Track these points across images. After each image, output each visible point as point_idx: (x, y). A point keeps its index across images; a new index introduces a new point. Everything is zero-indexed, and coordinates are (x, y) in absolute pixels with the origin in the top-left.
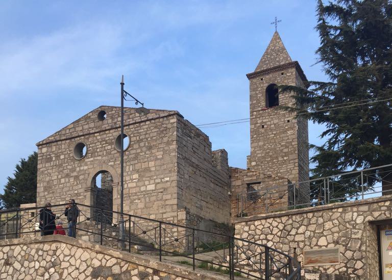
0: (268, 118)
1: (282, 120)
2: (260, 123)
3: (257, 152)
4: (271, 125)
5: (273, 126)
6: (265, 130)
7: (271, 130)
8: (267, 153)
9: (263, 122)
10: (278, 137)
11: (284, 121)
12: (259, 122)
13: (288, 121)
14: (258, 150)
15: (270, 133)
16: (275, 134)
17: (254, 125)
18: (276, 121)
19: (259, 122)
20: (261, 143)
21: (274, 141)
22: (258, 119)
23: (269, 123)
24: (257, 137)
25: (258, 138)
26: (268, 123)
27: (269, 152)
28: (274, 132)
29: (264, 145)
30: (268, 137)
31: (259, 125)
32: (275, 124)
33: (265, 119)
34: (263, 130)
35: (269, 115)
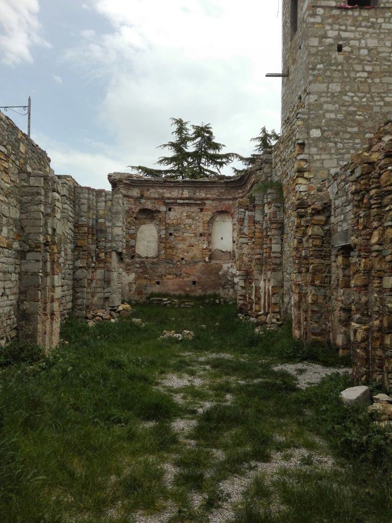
0: (352, 31)
4: (360, 48)
5: (364, 52)
6: (347, 58)
7: (361, 61)
9: (339, 38)
10: (377, 80)
12: (331, 34)
14: (327, 102)
15: (358, 68)
16: (369, 72)
18: (372, 43)
20: (335, 87)
21: (366, 89)
22: (328, 27)
23: (356, 43)
24: (325, 70)
25: (328, 73)
26: (352, 43)
28: (369, 68)
29: (343, 93)
30: (353, 75)
31: (329, 41)
32: (370, 50)
33: (346, 31)
34: (340, 57)
35: (356, 24)
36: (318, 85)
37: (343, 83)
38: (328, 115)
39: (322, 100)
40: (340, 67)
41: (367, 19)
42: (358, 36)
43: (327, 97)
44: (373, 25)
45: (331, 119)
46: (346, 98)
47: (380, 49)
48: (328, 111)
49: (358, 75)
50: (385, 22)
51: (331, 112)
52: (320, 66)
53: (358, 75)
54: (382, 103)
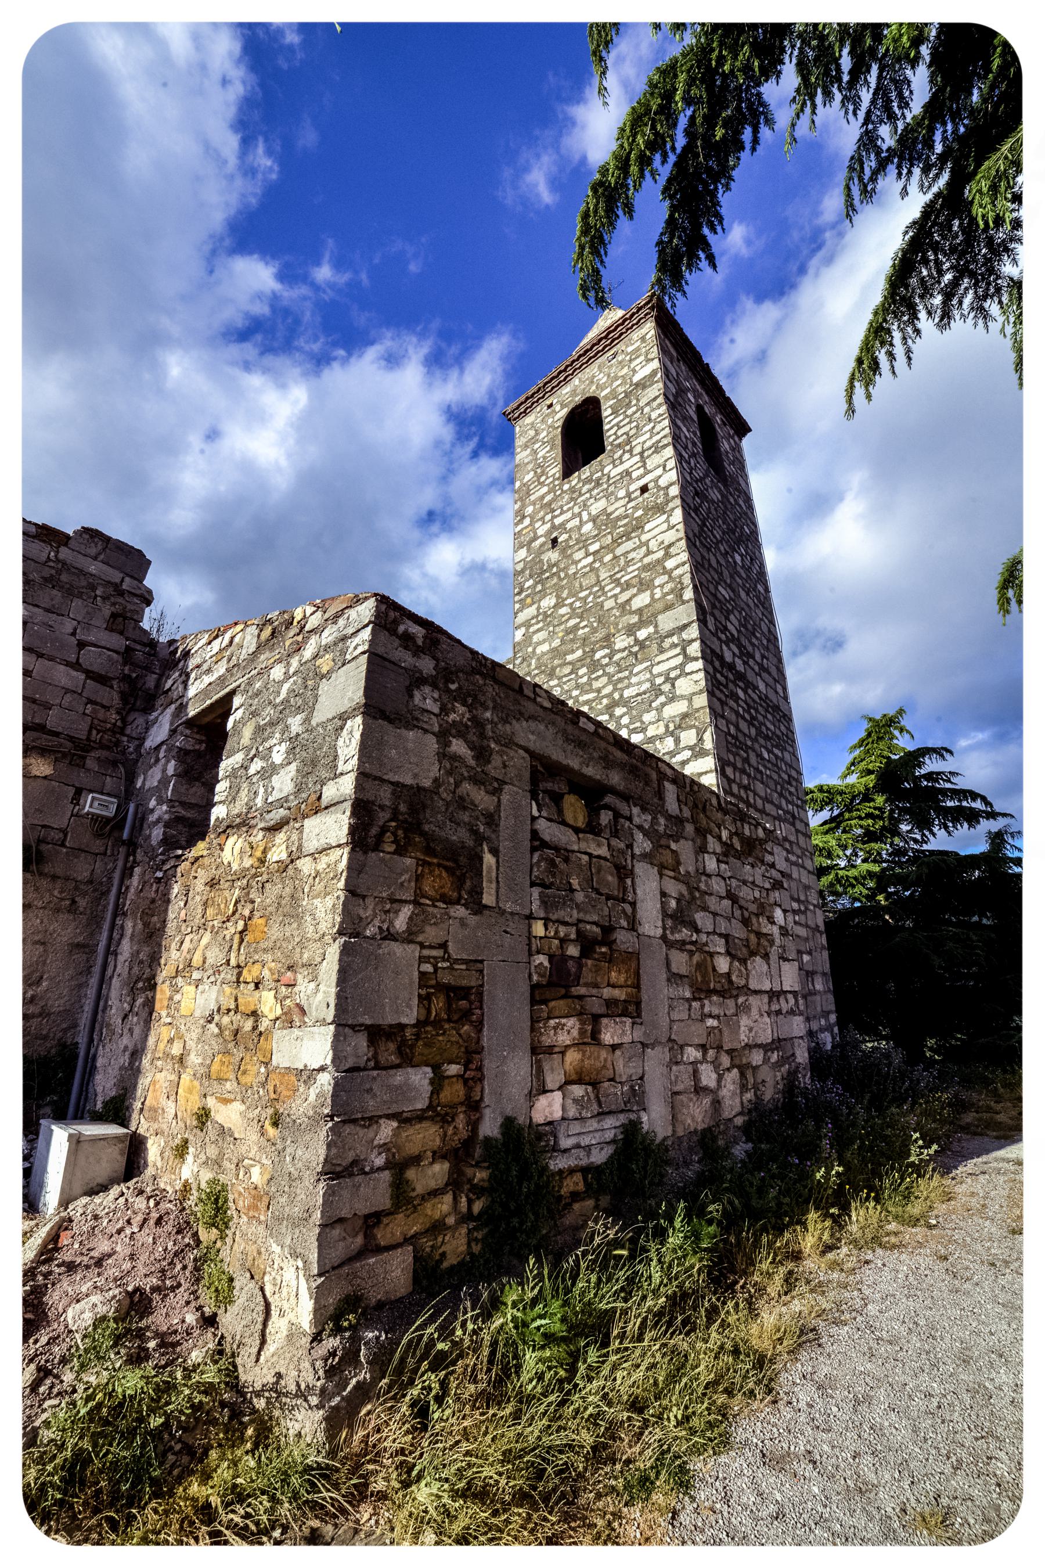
1: (622, 493)
2: (549, 532)
3: (535, 639)
4: (582, 523)
6: (563, 551)
7: (583, 543)
8: (568, 632)
11: (628, 495)
13: (644, 489)
14: (539, 630)
15: (580, 554)
16: (595, 553)
17: (525, 550)
18: (596, 508)
19: (540, 532)
23: (576, 522)
25: (539, 587)
26: (569, 526)
27: (576, 627)
28: (593, 548)
30: (572, 571)
31: (542, 539)
32: (594, 519)
34: (553, 556)
36: (526, 611)
37: (559, 589)
38: (538, 651)
39: (531, 630)
40: (555, 570)
41: (588, 481)
42: (576, 510)
43: (538, 622)
44: (598, 484)
45: (543, 654)
46: (563, 610)
47: (609, 510)
48: (539, 643)
49: (580, 566)
50: (615, 466)
51: (544, 641)
52: (531, 582)
53: (580, 566)
54: (618, 590)
